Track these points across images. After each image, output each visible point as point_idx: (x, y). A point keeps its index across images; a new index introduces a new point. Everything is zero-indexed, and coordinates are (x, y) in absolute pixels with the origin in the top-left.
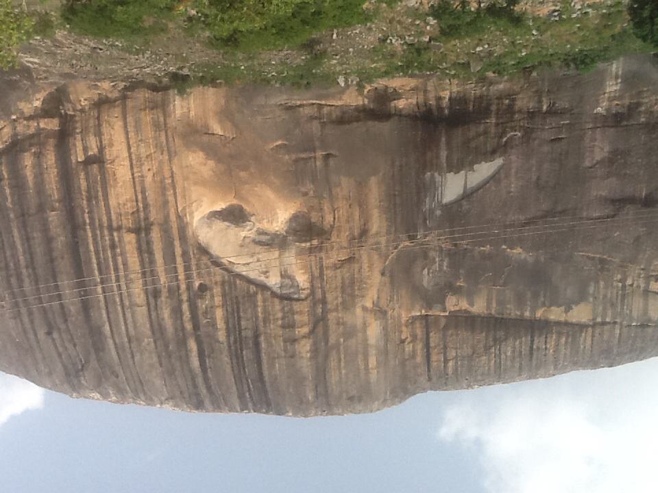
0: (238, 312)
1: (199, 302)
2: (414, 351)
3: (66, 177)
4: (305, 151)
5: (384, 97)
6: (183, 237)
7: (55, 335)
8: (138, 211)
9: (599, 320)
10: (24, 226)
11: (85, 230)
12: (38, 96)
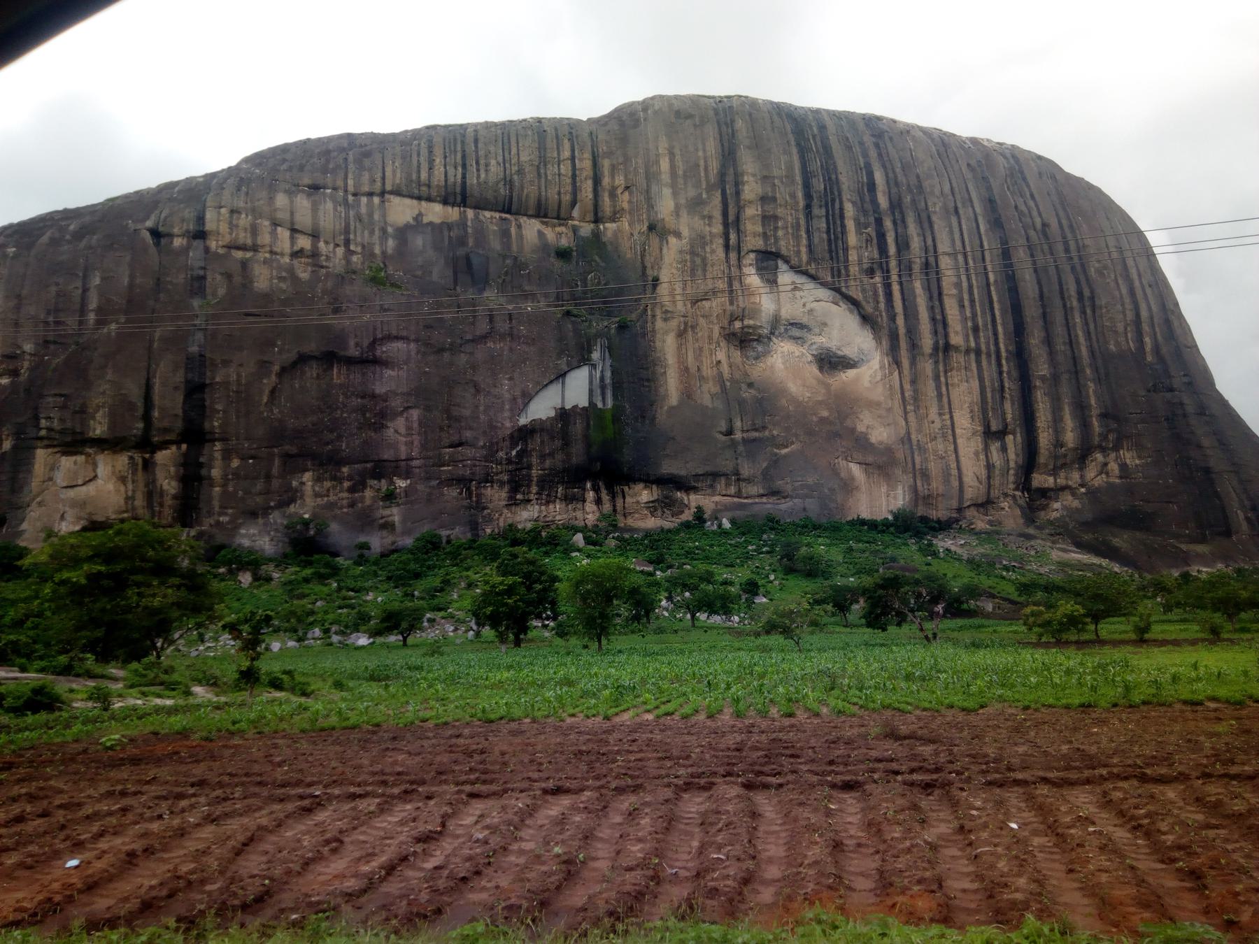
0: (829, 240)
1: (876, 255)
2: (613, 176)
4: (754, 440)
5: (665, 505)
6: (894, 337)
8: (946, 372)
9: (376, 200)
10: (1075, 360)
11: (1007, 351)
12: (1055, 515)
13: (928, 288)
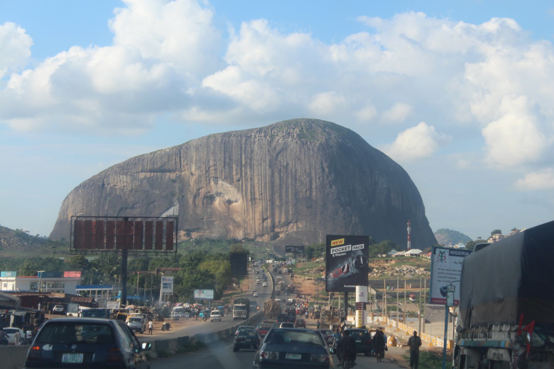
7: (285, 164)
13: (251, 185)
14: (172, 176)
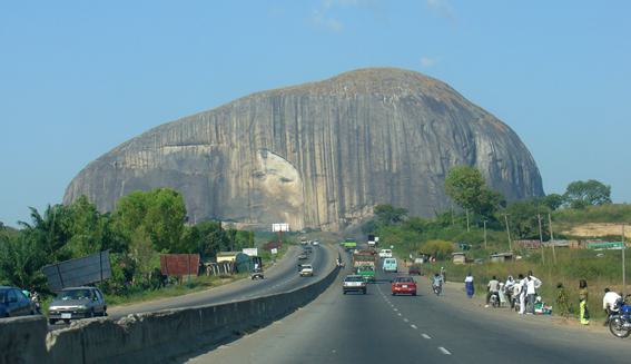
3: (342, 195)
6: (300, 172)
13: (311, 156)
14: (206, 150)
